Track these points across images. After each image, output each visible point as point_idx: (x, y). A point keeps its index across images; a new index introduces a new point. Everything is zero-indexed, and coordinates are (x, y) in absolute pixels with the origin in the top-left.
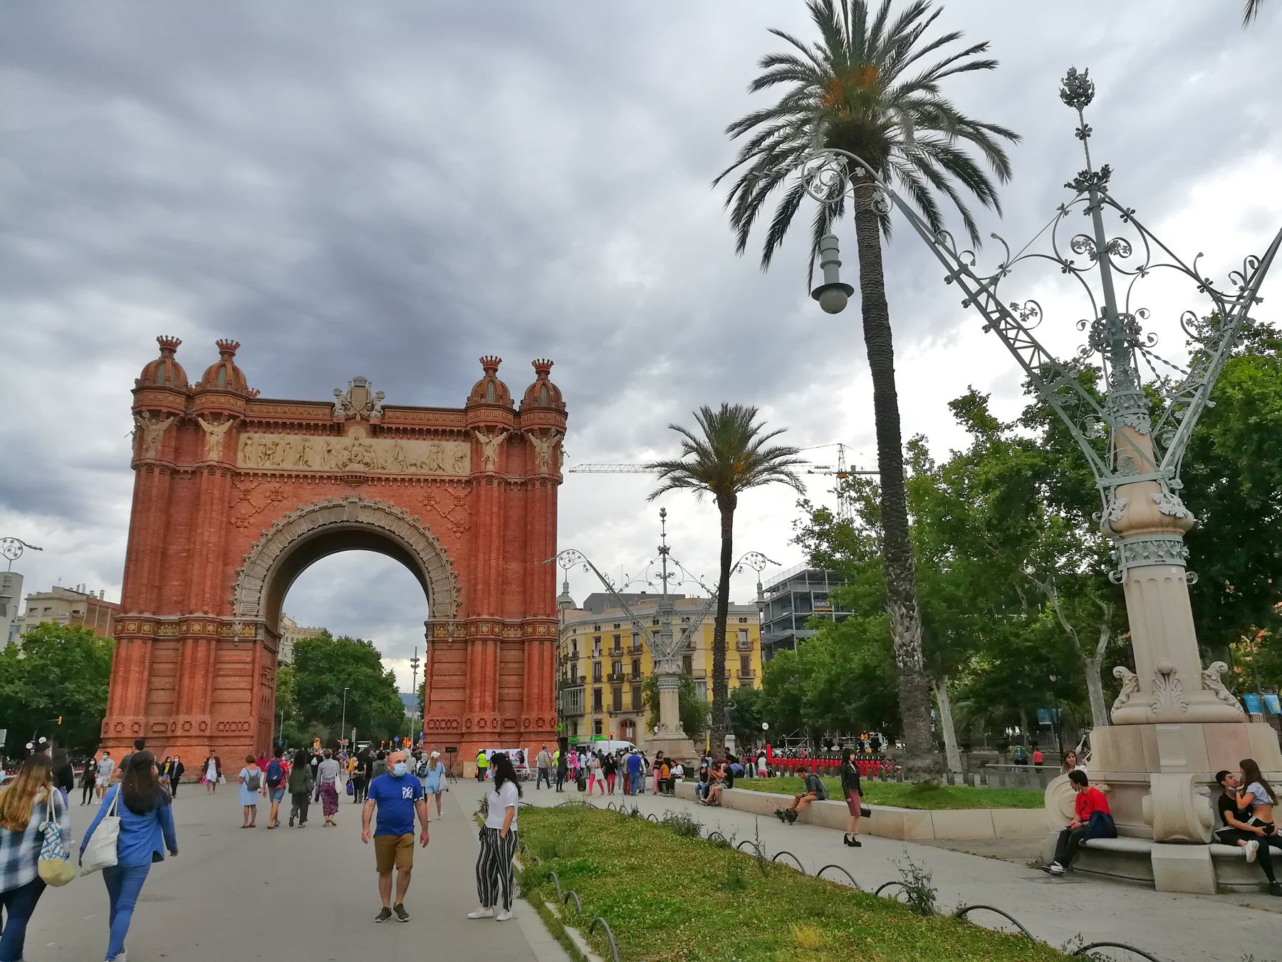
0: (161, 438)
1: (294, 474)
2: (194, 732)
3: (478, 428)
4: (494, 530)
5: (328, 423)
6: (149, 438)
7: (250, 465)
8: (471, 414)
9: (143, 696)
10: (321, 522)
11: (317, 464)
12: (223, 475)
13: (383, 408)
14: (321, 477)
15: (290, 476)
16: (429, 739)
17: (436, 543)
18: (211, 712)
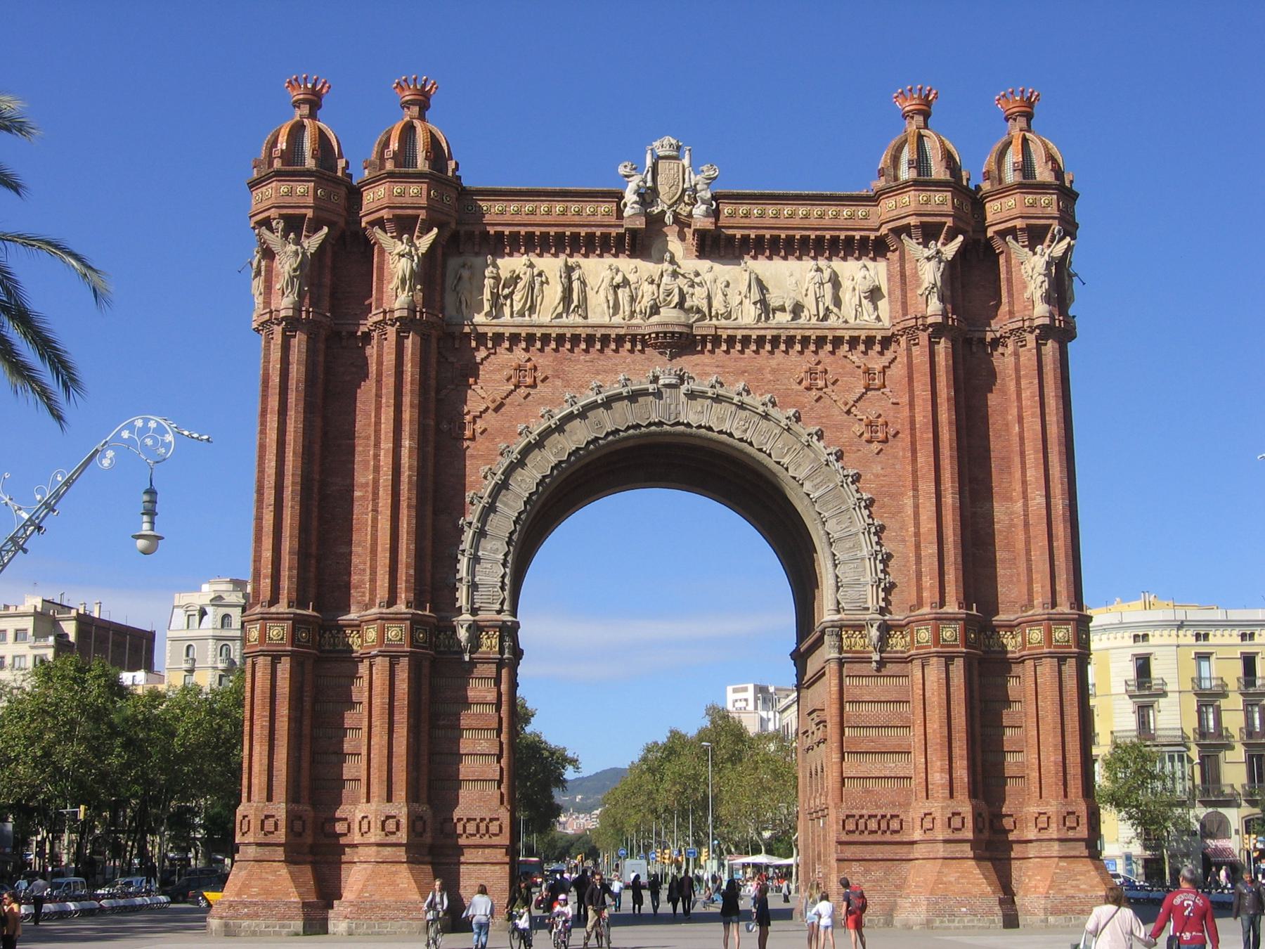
0: (307, 269)
1: (554, 332)
3: (906, 229)
5: (614, 231)
9: (305, 765)
11: (599, 314)
14: (605, 340)
16: (850, 852)
18: (430, 802)
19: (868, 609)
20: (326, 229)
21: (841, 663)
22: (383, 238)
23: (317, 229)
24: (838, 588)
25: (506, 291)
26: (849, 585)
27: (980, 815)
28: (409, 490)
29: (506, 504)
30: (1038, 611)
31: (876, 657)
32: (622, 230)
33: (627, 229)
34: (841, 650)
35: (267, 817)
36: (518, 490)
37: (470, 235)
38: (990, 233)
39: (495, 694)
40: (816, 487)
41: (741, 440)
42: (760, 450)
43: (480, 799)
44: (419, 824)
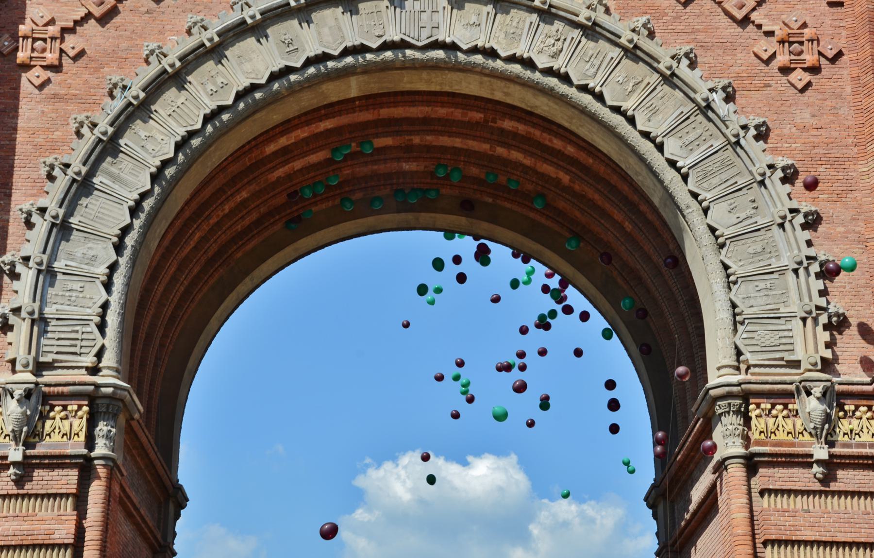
10: (313, 50)
19: (796, 364)
21: (751, 464)
29: (115, 178)
31: (821, 453)
36: (143, 154)
39: (71, 527)
40: (688, 147)
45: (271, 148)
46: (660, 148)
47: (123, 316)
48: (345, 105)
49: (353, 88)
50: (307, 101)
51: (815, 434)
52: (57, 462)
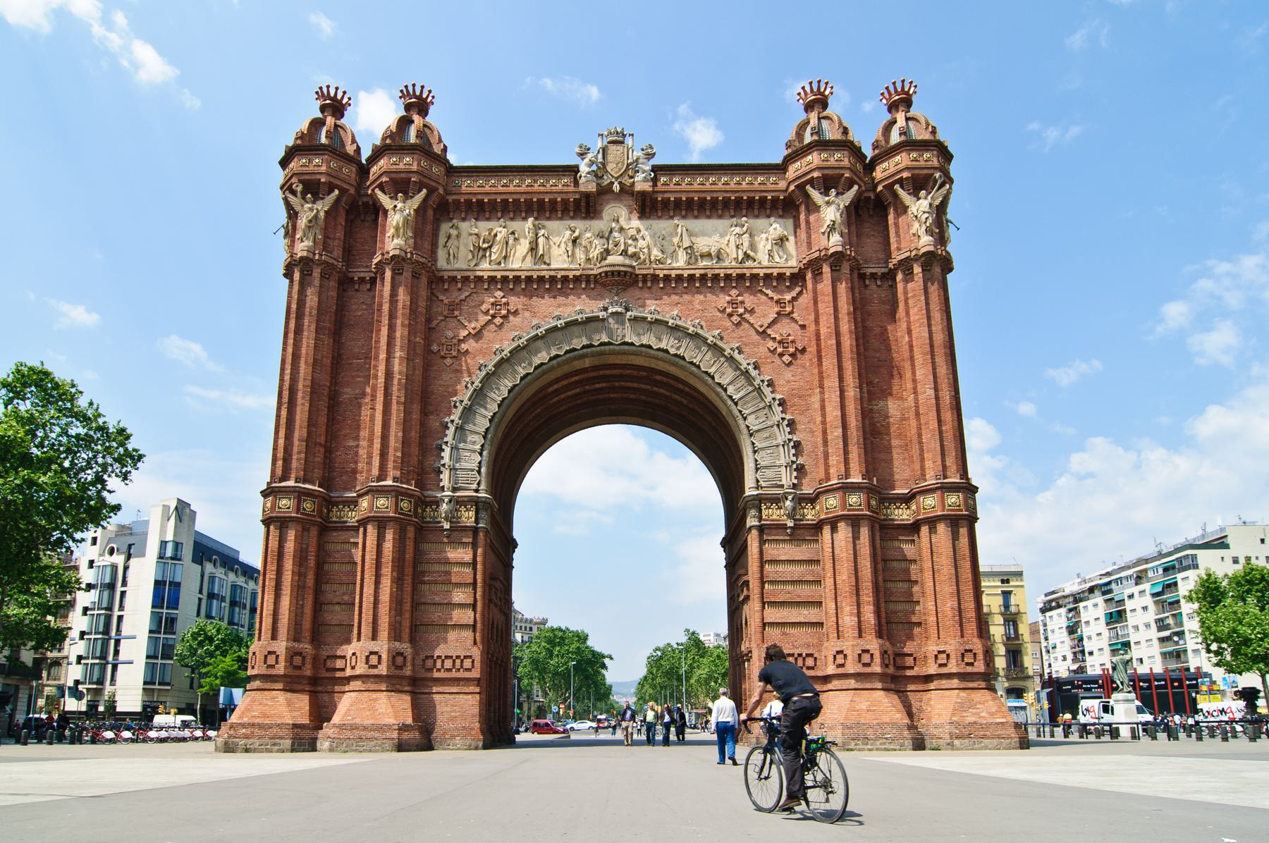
1: (523, 275)
2: (383, 670)
4: (847, 342)
6: (302, 222)
7: (457, 266)
8: (794, 170)
11: (560, 260)
12: (416, 276)
13: (656, 169)
14: (565, 279)
15: (517, 279)
17: (754, 373)
18: (412, 640)
19: (782, 486)
20: (337, 192)
21: (761, 529)
22: (384, 200)
23: (331, 191)
24: (757, 469)
25: (485, 245)
26: (766, 467)
27: (886, 652)
28: (399, 390)
30: (931, 481)
31: (790, 523)
32: (577, 196)
33: (582, 193)
34: (760, 519)
35: (270, 653)
37: (457, 202)
38: (880, 188)
40: (738, 390)
41: (676, 355)
42: (692, 363)
43: (459, 645)
44: (399, 660)
45: (550, 390)
46: (725, 390)
47: (488, 467)
48: (584, 370)
49: (587, 363)
50: (566, 369)
51: (789, 516)
52: (465, 529)
